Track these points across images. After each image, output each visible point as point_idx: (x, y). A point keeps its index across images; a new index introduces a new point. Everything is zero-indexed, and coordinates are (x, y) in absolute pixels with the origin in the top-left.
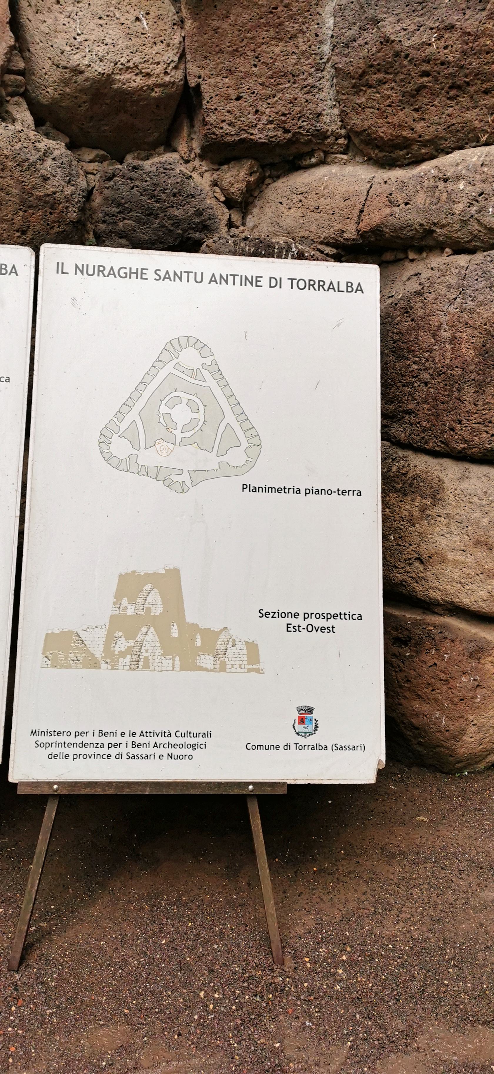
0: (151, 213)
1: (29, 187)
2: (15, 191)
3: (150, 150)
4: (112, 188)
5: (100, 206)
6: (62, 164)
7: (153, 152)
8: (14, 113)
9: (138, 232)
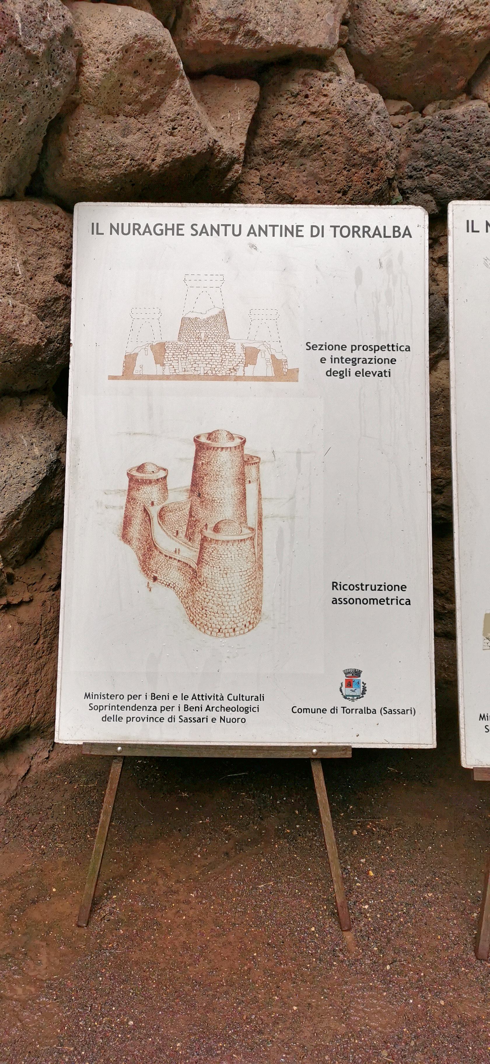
0: (462, 165)
1: (356, 143)
2: (342, 149)
3: (450, 97)
4: (422, 140)
5: (406, 161)
6: (385, 118)
7: (455, 101)
8: (340, 65)
9: (445, 186)
